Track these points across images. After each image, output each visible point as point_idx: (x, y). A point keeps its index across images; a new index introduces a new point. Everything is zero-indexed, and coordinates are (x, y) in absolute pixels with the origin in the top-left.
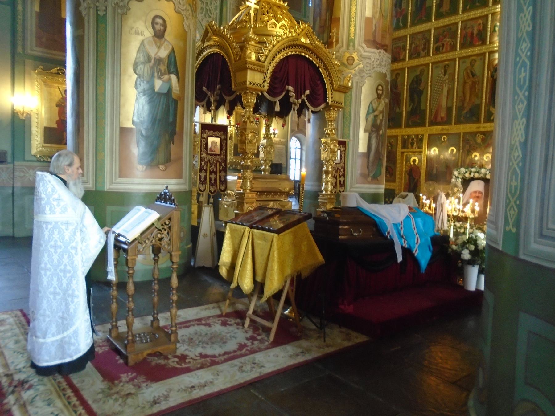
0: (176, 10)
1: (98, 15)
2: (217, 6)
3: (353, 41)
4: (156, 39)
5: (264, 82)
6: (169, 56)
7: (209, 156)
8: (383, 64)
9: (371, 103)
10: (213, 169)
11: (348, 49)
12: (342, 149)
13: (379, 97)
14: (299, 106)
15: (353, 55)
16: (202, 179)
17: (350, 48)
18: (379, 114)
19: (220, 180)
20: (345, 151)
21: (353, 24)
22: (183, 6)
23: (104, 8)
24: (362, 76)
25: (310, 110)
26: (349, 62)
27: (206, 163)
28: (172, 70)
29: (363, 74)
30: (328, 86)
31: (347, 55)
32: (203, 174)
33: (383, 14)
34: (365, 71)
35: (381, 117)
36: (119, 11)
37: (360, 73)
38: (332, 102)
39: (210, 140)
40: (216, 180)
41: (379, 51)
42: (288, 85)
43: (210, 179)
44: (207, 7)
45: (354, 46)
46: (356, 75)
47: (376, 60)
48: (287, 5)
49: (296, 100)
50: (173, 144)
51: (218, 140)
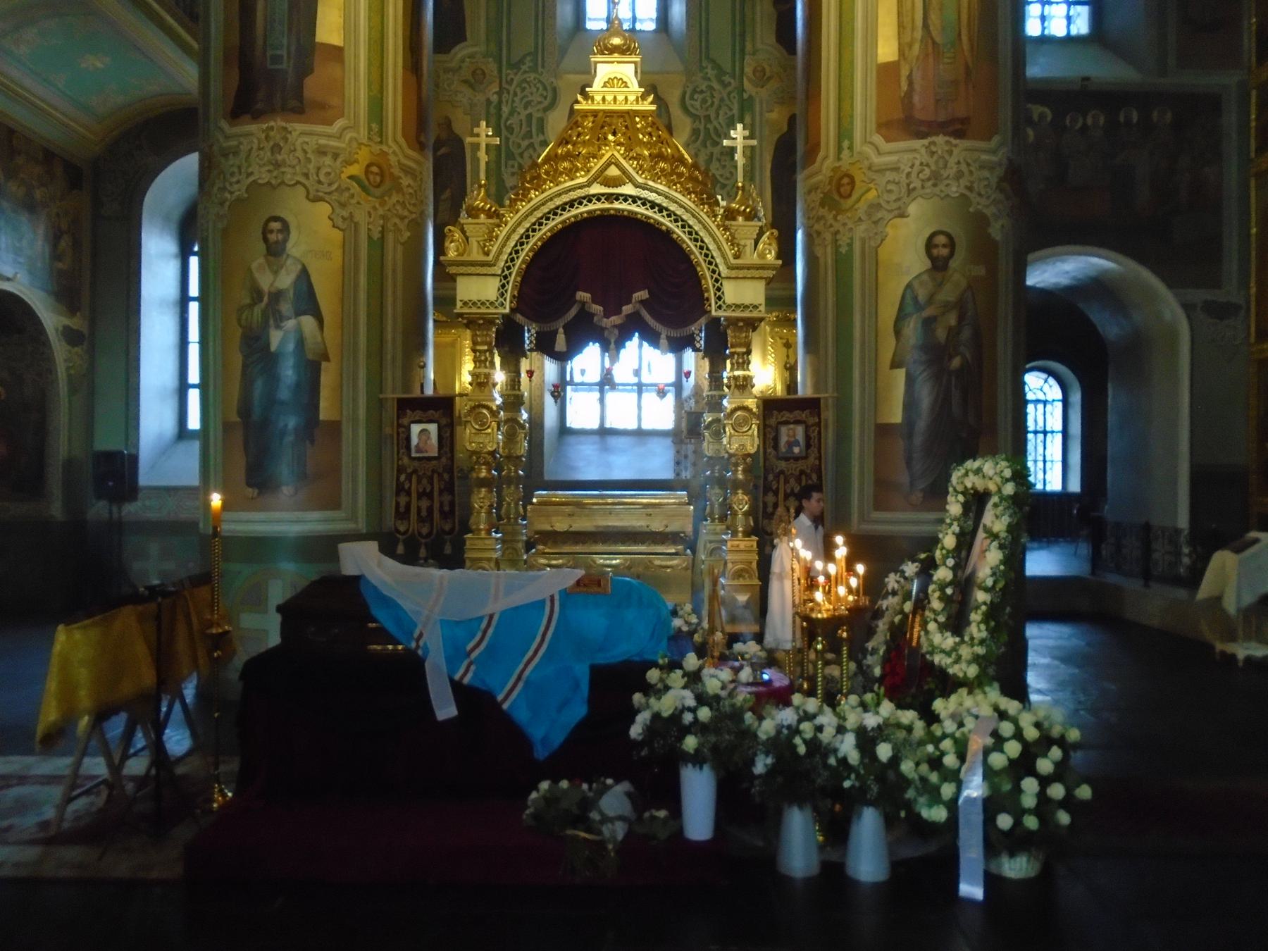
2: (733, 115)
5: (502, 295)
7: (416, 463)
8: (952, 170)
9: (909, 286)
10: (425, 489)
11: (839, 159)
12: (812, 420)
13: (938, 265)
14: (616, 332)
15: (851, 172)
16: (402, 510)
17: (842, 156)
18: (943, 314)
19: (442, 512)
20: (819, 424)
22: (330, 185)
24: (875, 219)
25: (663, 336)
26: (842, 190)
27: (409, 478)
29: (879, 215)
30: (704, 269)
32: (403, 500)
33: (938, 40)
34: (884, 204)
35: (952, 319)
37: (869, 215)
39: (416, 429)
40: (430, 510)
41: (926, 142)
42: (578, 289)
43: (419, 509)
44: (709, 126)
45: (851, 148)
46: (860, 218)
47: (917, 168)
49: (605, 320)
50: (312, 442)
51: (433, 428)
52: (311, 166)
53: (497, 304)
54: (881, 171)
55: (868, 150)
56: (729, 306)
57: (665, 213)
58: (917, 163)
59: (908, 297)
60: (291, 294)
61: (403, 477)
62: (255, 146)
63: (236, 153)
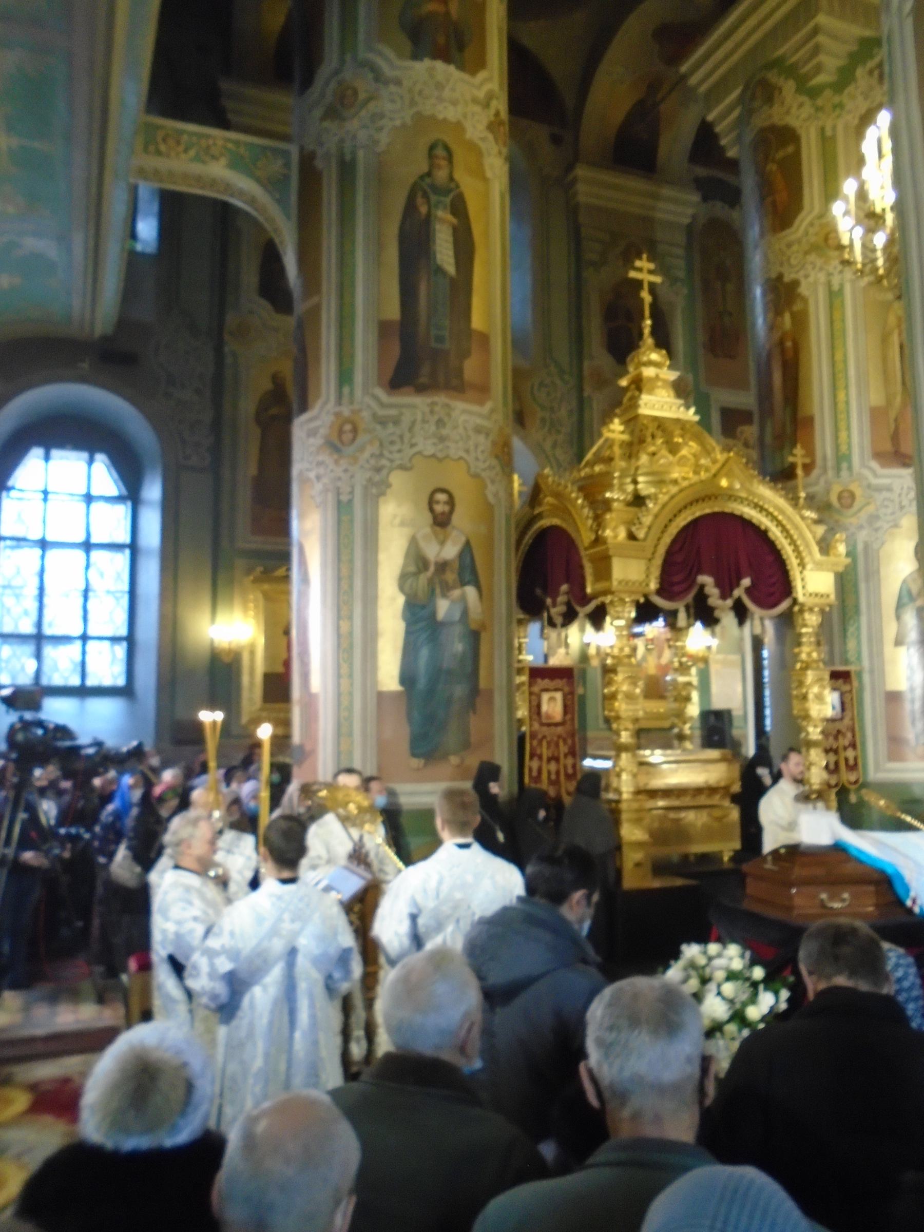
0: (473, 470)
1: (339, 502)
3: (848, 458)
4: (438, 529)
6: (461, 555)
9: (904, 582)
16: (535, 774)
20: (851, 691)
21: (842, 425)
23: (349, 489)
26: (843, 501)
28: (468, 577)
30: (792, 562)
31: (836, 489)
32: (535, 764)
36: (374, 491)
38: (804, 595)
45: (850, 468)
47: (905, 491)
48: (696, 413)
50: (475, 713)
52: (471, 443)
53: (644, 584)
54: (879, 489)
55: (866, 473)
56: (811, 595)
57: (764, 513)
58: (905, 486)
59: (905, 593)
60: (456, 565)
61: (535, 743)
62: (419, 417)
63: (396, 422)
